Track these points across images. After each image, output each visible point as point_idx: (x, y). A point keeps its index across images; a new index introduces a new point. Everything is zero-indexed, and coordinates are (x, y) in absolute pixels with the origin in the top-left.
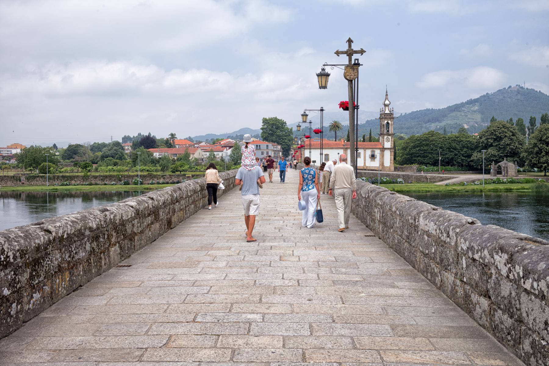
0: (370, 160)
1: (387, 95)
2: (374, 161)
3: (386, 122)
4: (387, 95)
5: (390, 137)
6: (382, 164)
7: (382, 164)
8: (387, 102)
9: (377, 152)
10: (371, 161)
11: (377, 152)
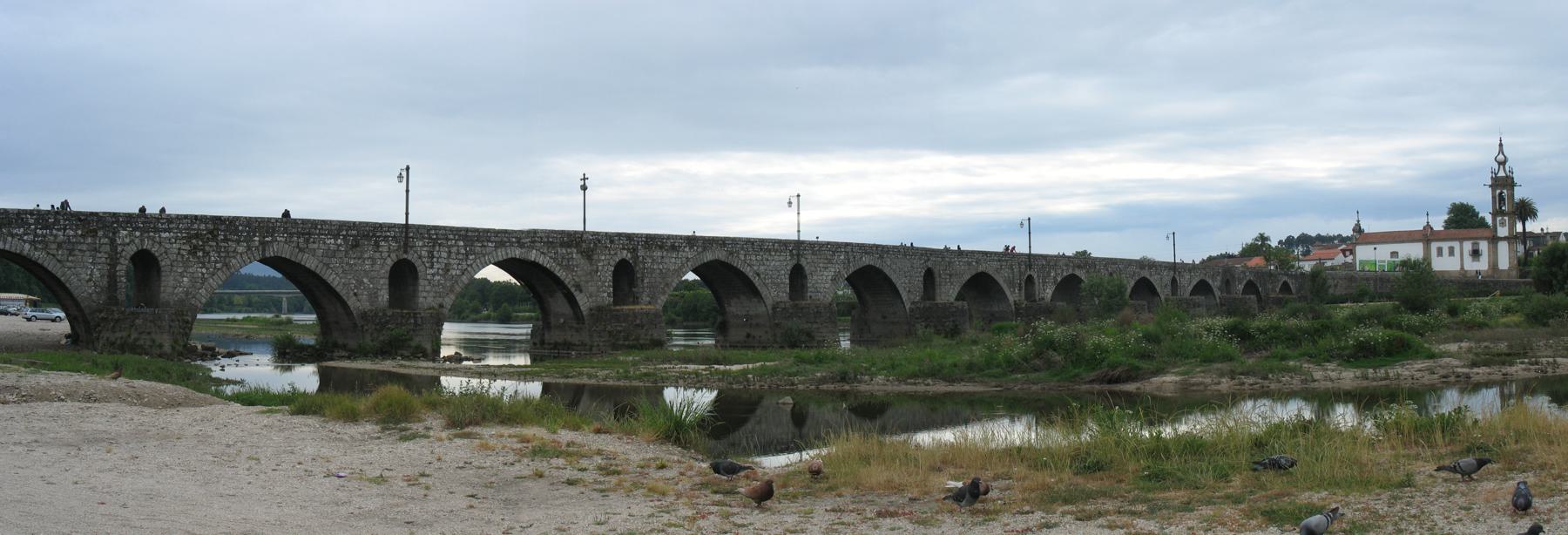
0: (1470, 258)
1: (1501, 145)
2: (1479, 261)
3: (1498, 191)
4: (1501, 145)
5: (1506, 218)
6: (1494, 265)
7: (1494, 265)
8: (1501, 157)
9: (1484, 246)
10: (1473, 261)
11: (1484, 246)
